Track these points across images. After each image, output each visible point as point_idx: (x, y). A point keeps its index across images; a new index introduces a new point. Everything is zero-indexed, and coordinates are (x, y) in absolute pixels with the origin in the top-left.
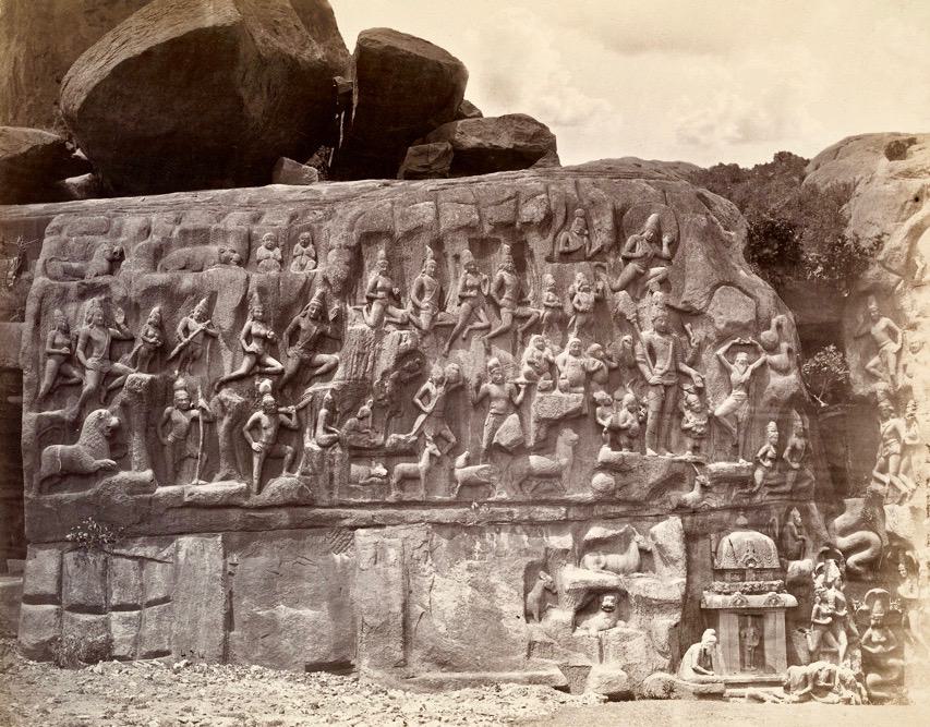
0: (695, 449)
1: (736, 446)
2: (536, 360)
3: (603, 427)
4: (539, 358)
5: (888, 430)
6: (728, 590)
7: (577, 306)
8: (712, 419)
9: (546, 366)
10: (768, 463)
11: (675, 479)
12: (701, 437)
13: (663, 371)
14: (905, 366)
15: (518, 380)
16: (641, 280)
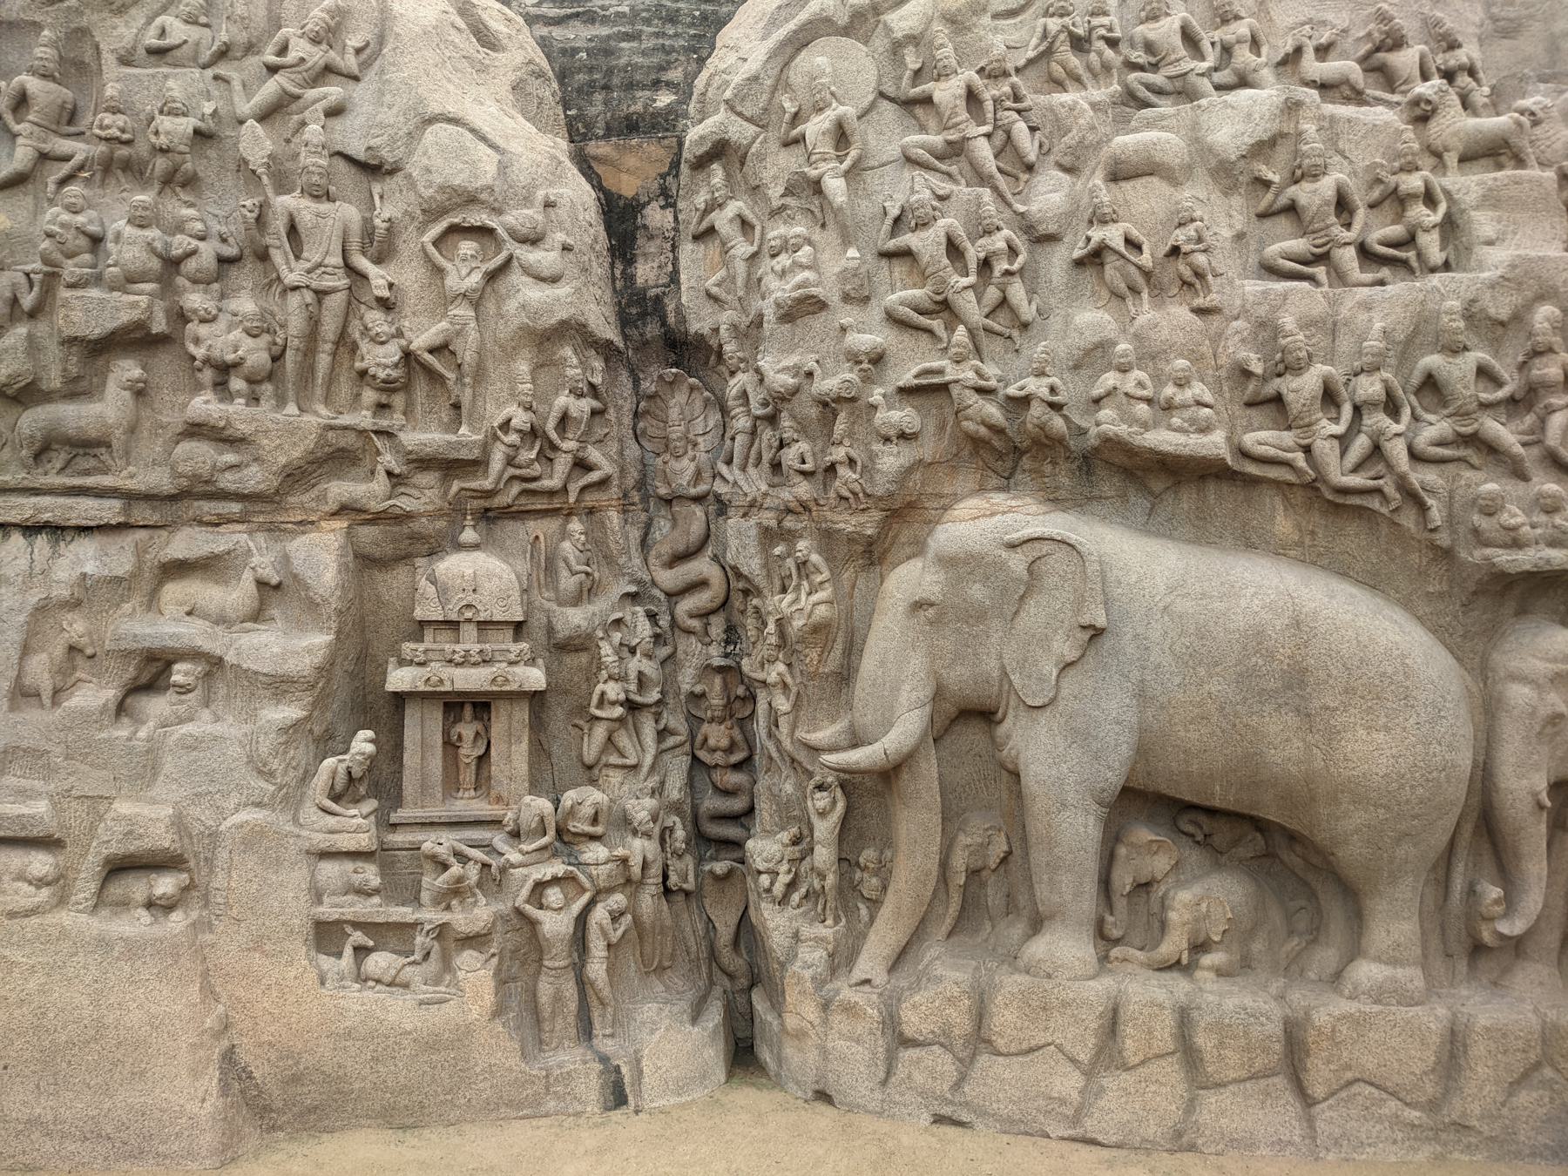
0: (382, 407)
1: (457, 406)
2: (56, 229)
3: (194, 358)
4: (62, 225)
5: (734, 391)
6: (422, 658)
7: (153, 139)
8: (408, 356)
9: (83, 242)
10: (513, 438)
11: (337, 457)
12: (388, 386)
13: (308, 265)
14: (760, 280)
15: (28, 268)
16: (294, 107)
